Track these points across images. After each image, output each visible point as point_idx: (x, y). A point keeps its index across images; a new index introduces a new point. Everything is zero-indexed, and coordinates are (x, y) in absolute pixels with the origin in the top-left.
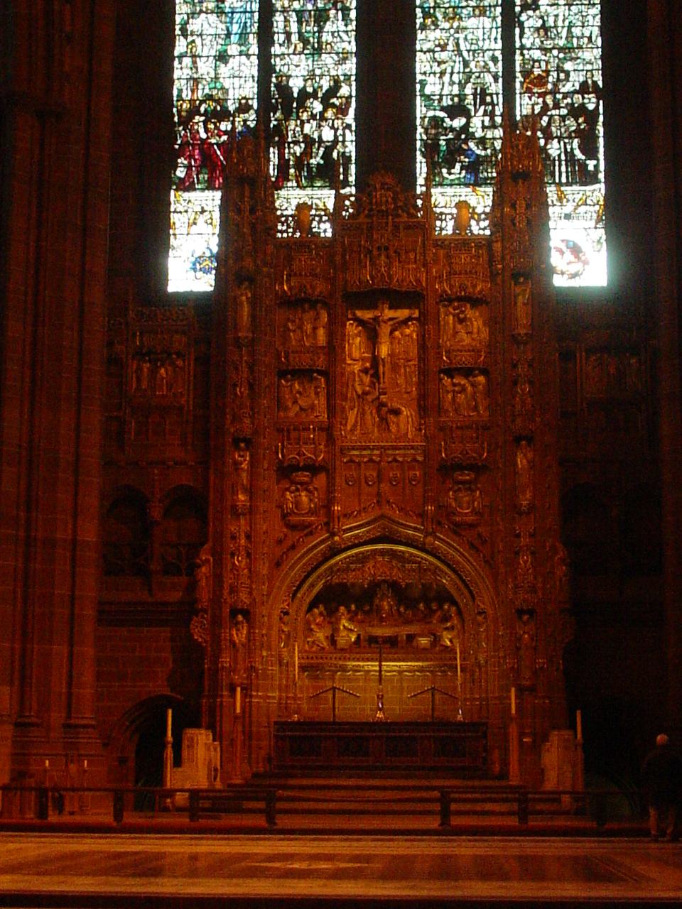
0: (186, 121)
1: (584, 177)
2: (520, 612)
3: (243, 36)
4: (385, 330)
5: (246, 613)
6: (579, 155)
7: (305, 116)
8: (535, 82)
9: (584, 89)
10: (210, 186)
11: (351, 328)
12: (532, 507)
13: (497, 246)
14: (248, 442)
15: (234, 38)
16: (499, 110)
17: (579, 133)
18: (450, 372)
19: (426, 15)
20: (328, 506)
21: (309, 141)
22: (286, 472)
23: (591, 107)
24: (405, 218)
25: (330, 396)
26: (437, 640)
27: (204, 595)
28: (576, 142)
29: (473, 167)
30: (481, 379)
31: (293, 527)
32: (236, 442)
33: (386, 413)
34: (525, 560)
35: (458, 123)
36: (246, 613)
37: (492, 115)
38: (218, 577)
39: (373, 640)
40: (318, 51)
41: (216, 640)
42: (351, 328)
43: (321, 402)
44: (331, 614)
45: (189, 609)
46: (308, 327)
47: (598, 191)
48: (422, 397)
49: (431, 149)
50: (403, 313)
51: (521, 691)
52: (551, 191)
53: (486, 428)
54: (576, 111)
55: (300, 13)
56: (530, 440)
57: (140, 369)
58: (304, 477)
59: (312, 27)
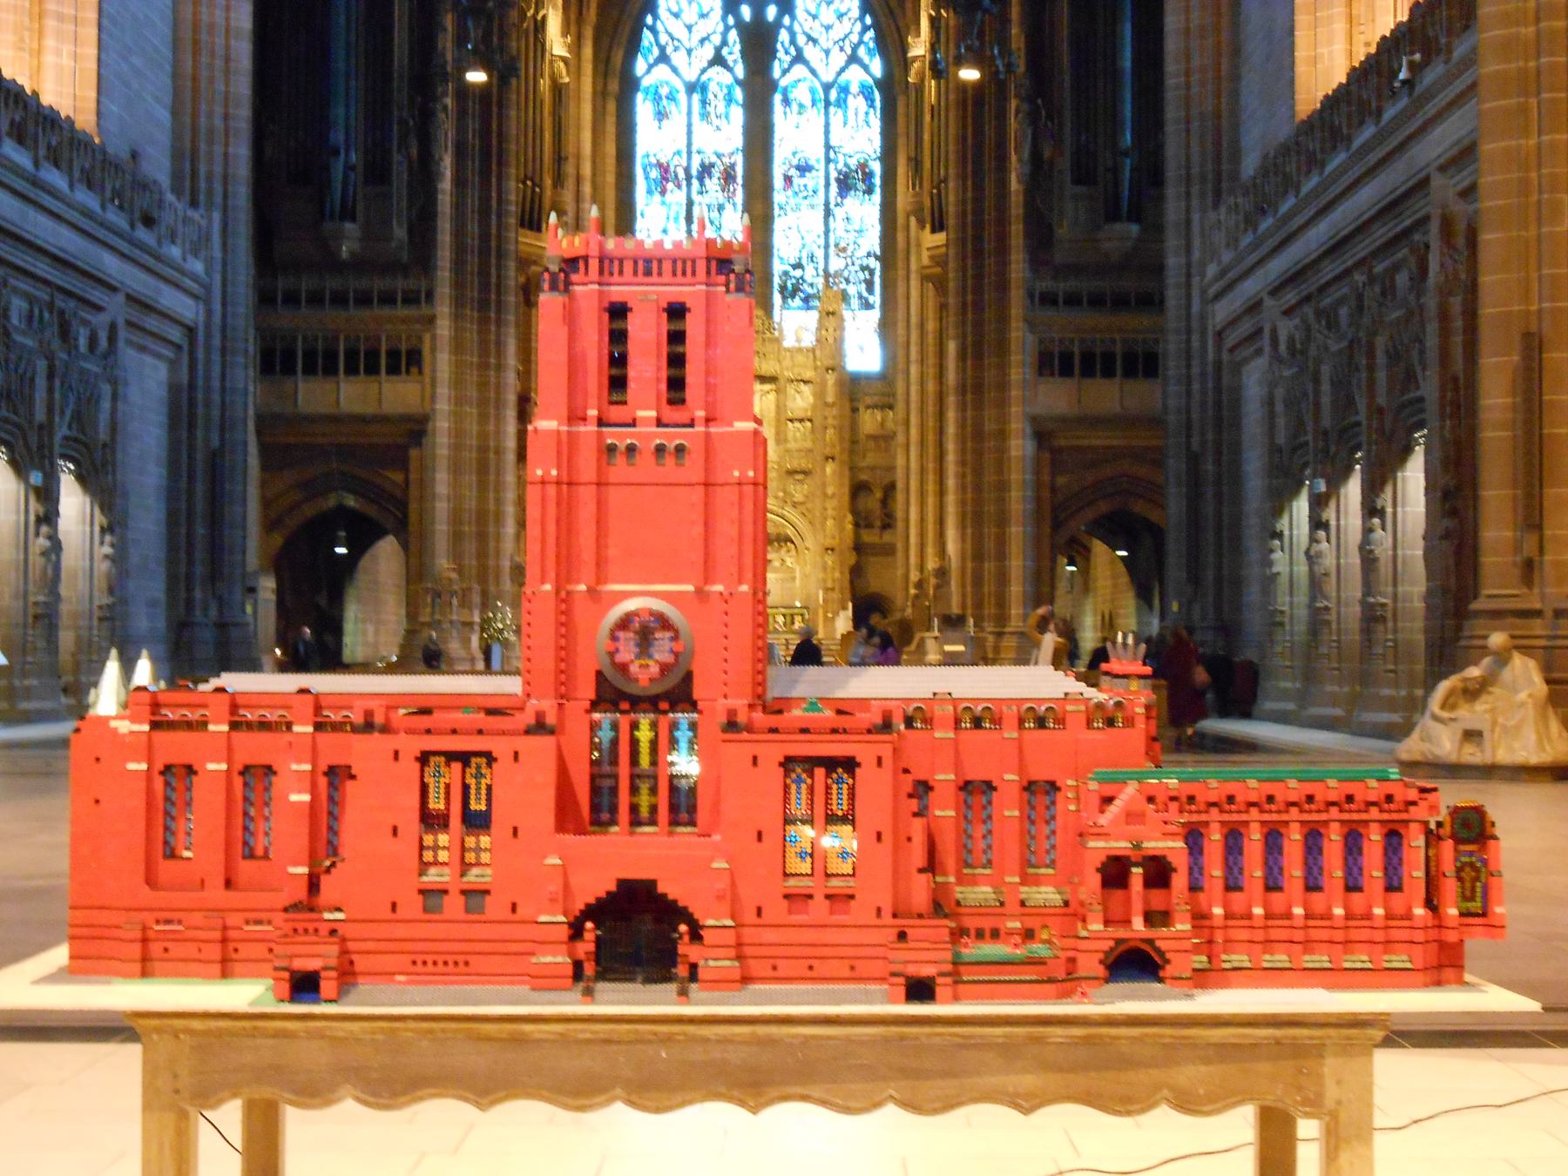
1: (867, 306)
3: (676, 219)
6: (865, 294)
9: (869, 255)
12: (834, 495)
15: (671, 220)
16: (821, 266)
17: (866, 281)
18: (791, 421)
19: (781, 208)
23: (872, 266)
24: (768, 335)
28: (863, 286)
29: (806, 300)
35: (798, 273)
37: (816, 269)
47: (875, 315)
49: (783, 289)
50: (767, 387)
51: (826, 590)
52: (847, 314)
53: (810, 451)
54: (863, 268)
55: (709, 206)
56: (833, 458)
59: (715, 215)
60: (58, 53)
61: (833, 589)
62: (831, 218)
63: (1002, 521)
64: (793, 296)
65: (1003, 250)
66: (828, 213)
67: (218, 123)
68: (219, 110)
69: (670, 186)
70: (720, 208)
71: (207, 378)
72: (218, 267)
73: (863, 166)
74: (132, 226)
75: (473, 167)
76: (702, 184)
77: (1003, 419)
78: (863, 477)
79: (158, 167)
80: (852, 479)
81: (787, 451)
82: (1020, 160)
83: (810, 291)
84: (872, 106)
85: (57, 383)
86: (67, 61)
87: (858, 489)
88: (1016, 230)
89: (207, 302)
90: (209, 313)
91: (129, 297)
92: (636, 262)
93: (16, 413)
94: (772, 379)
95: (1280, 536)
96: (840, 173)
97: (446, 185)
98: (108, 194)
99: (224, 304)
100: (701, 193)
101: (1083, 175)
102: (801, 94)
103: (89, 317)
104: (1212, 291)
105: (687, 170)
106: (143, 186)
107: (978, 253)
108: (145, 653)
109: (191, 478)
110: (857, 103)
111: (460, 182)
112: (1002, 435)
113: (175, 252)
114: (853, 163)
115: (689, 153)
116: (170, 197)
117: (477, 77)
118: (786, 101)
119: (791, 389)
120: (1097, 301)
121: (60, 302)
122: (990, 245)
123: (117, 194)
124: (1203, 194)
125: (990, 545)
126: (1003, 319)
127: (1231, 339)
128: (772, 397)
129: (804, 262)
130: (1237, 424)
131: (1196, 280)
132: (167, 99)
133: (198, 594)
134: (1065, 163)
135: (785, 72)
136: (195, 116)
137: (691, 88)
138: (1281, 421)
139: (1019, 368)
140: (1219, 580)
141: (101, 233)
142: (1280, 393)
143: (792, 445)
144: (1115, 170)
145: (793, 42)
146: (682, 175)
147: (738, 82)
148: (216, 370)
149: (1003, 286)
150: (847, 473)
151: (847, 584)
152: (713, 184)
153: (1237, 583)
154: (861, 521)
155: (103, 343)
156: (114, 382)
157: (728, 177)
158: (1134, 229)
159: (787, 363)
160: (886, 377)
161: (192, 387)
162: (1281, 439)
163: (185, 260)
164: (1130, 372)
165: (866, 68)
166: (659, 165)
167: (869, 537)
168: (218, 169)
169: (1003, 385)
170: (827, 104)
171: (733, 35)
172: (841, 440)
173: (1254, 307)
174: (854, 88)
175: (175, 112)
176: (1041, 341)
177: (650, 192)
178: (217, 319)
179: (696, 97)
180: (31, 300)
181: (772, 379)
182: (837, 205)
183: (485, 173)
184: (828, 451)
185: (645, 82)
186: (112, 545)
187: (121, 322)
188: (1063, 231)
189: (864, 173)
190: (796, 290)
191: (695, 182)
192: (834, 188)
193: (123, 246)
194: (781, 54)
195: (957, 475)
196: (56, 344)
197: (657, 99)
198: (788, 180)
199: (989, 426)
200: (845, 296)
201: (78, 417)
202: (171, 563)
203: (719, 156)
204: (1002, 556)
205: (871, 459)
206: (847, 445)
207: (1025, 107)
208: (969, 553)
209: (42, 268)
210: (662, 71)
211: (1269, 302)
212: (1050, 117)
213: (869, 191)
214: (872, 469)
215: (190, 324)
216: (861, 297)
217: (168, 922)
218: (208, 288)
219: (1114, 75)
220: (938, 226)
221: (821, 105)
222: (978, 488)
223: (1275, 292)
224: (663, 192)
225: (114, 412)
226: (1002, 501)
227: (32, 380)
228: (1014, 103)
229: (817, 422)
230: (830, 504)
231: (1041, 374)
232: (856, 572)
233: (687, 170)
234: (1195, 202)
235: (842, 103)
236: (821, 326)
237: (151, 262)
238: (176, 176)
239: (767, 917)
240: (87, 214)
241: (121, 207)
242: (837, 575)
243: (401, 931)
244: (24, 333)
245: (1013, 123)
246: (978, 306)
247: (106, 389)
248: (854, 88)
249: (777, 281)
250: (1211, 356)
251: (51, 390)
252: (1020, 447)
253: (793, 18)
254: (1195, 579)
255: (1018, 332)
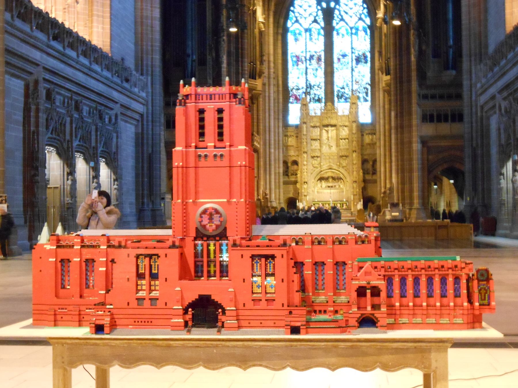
0: (292, 91)
1: (366, 100)
2: (354, 182)
4: (330, 132)
5: (306, 183)
6: (365, 96)
7: (314, 89)
8: (357, 82)
10: (297, 103)
11: (324, 131)
12: (356, 164)
13: (350, 116)
14: (306, 152)
18: (341, 139)
20: (320, 163)
21: (315, 94)
22: (313, 157)
25: (320, 143)
26: (339, 186)
27: (299, 180)
29: (346, 99)
30: (347, 140)
31: (314, 167)
32: (304, 152)
33: (330, 147)
34: (355, 173)
35: (343, 90)
36: (306, 183)
38: (301, 177)
39: (329, 187)
40: (316, 76)
41: (301, 187)
42: (324, 131)
43: (319, 145)
44: (321, 181)
45: (296, 182)
46: (316, 131)
47: (369, 103)
48: (337, 144)
49: (338, 96)
50: (333, 128)
51: (354, 195)
52: (359, 103)
53: (348, 149)
54: (365, 88)
56: (355, 151)
57: (285, 139)
58: (315, 158)
59: (315, 71)
60: (98, 27)
61: (356, 195)
62: (353, 72)
63: (411, 171)
64: (341, 98)
65: (409, 81)
66: (352, 70)
67: (150, 48)
68: (150, 44)
69: (300, 63)
70: (317, 70)
71: (147, 131)
72: (150, 94)
73: (364, 54)
74: (122, 82)
75: (233, 58)
76: (310, 62)
77: (410, 138)
78: (366, 157)
79: (130, 63)
80: (362, 158)
81: (340, 149)
82: (415, 50)
83: (347, 96)
84: (366, 34)
85: (99, 133)
86: (100, 30)
87: (364, 162)
88: (414, 74)
89: (147, 105)
90: (148, 109)
91: (121, 105)
92: (207, 96)
93: (85, 143)
94: (334, 126)
95: (503, 175)
96: (356, 56)
97: (224, 65)
98: (114, 72)
99: (152, 106)
100: (310, 65)
101: (436, 55)
102: (342, 31)
103: (109, 112)
104: (479, 92)
105: (305, 58)
106: (125, 69)
107: (401, 82)
108: (46, 224)
109: (143, 162)
110: (361, 33)
111: (229, 64)
112: (410, 143)
113: (136, 90)
114: (361, 53)
115: (306, 52)
116: (134, 72)
117: (233, 30)
118: (338, 34)
119: (341, 129)
120: (441, 97)
121: (99, 108)
122: (405, 79)
123: (117, 72)
124: (475, 60)
125: (407, 179)
126: (410, 103)
127: (486, 109)
128: (335, 131)
129: (345, 86)
130: (488, 137)
131: (473, 89)
132: (133, 41)
133: (145, 200)
134: (429, 52)
135: (337, 24)
136: (142, 46)
137: (306, 30)
138: (503, 136)
139: (416, 119)
140: (483, 189)
141: (112, 85)
142: (502, 127)
143: (342, 147)
144: (447, 53)
145: (340, 14)
146: (303, 59)
147: (322, 28)
148: (150, 127)
149: (409, 93)
150: (360, 156)
151: (361, 193)
152: (314, 62)
153: (489, 191)
154: (365, 172)
155: (113, 120)
156: (117, 132)
157: (319, 59)
158: (454, 72)
159: (339, 120)
160: (373, 124)
161: (142, 133)
162: (503, 141)
163: (139, 92)
164: (453, 120)
165: (364, 21)
166: (296, 56)
167: (368, 177)
168: (150, 63)
169: (410, 126)
170: (352, 34)
171: (320, 13)
172: (358, 145)
173: (493, 98)
174: (361, 28)
175: (136, 44)
176: (423, 111)
177: (293, 65)
178: (150, 111)
179: (308, 33)
180: (90, 107)
181: (334, 126)
182: (356, 67)
183: (237, 61)
184: (354, 149)
185: (291, 29)
186: (117, 185)
187: (119, 113)
188: (430, 74)
189: (364, 56)
190: (342, 96)
191: (308, 62)
192: (354, 62)
193: (119, 89)
194: (336, 18)
195: (395, 156)
196: (98, 121)
197: (295, 34)
198: (339, 59)
199: (406, 140)
200: (358, 98)
201: (105, 144)
202: (137, 190)
203: (316, 52)
204: (411, 183)
205: (368, 151)
206: (360, 147)
207: (416, 33)
208: (400, 181)
209: (93, 97)
210: (297, 25)
211: (498, 96)
212: (424, 36)
213: (366, 62)
214: (369, 155)
215: (142, 113)
216: (364, 98)
217: (62, 309)
218: (147, 102)
219: (446, 21)
220: (388, 73)
221: (350, 34)
222: (402, 160)
223: (500, 91)
224: (297, 65)
225: (117, 142)
226: (411, 164)
227: (90, 133)
228: (412, 32)
229: (350, 139)
230: (355, 167)
231: (423, 122)
232: (364, 189)
233: (305, 58)
234: (473, 62)
235: (356, 34)
236: (351, 108)
237: (128, 94)
238: (136, 65)
239: (247, 306)
240: (107, 78)
241: (118, 76)
242: (358, 190)
243: (131, 311)
244: (88, 118)
245: (412, 38)
246: (402, 100)
247: (115, 135)
248: (361, 28)
249: (336, 93)
250: (479, 114)
251: (96, 136)
252: (416, 146)
253: (339, 5)
254: (475, 189)
255: (415, 108)
